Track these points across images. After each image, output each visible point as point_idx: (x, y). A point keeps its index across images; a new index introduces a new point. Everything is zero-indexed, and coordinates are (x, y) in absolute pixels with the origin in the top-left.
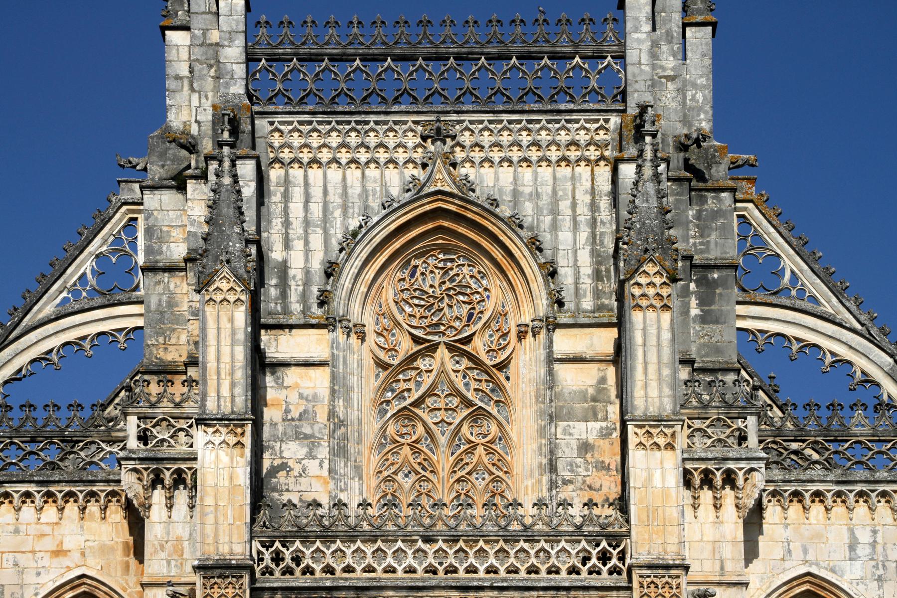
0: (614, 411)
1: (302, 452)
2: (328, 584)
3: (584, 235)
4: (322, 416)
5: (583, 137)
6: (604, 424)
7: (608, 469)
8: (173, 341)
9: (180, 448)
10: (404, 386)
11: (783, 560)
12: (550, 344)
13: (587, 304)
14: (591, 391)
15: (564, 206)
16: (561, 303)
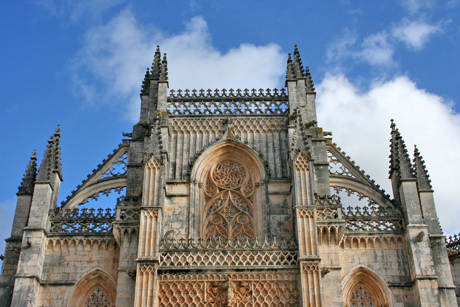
0: (290, 211)
1: (179, 226)
2: (186, 268)
3: (277, 154)
4: (186, 214)
5: (275, 124)
6: (286, 216)
7: (288, 231)
8: (136, 189)
9: (133, 221)
10: (216, 205)
11: (352, 263)
12: (267, 188)
13: (279, 176)
14: (281, 204)
15: (270, 145)
16: (270, 175)
